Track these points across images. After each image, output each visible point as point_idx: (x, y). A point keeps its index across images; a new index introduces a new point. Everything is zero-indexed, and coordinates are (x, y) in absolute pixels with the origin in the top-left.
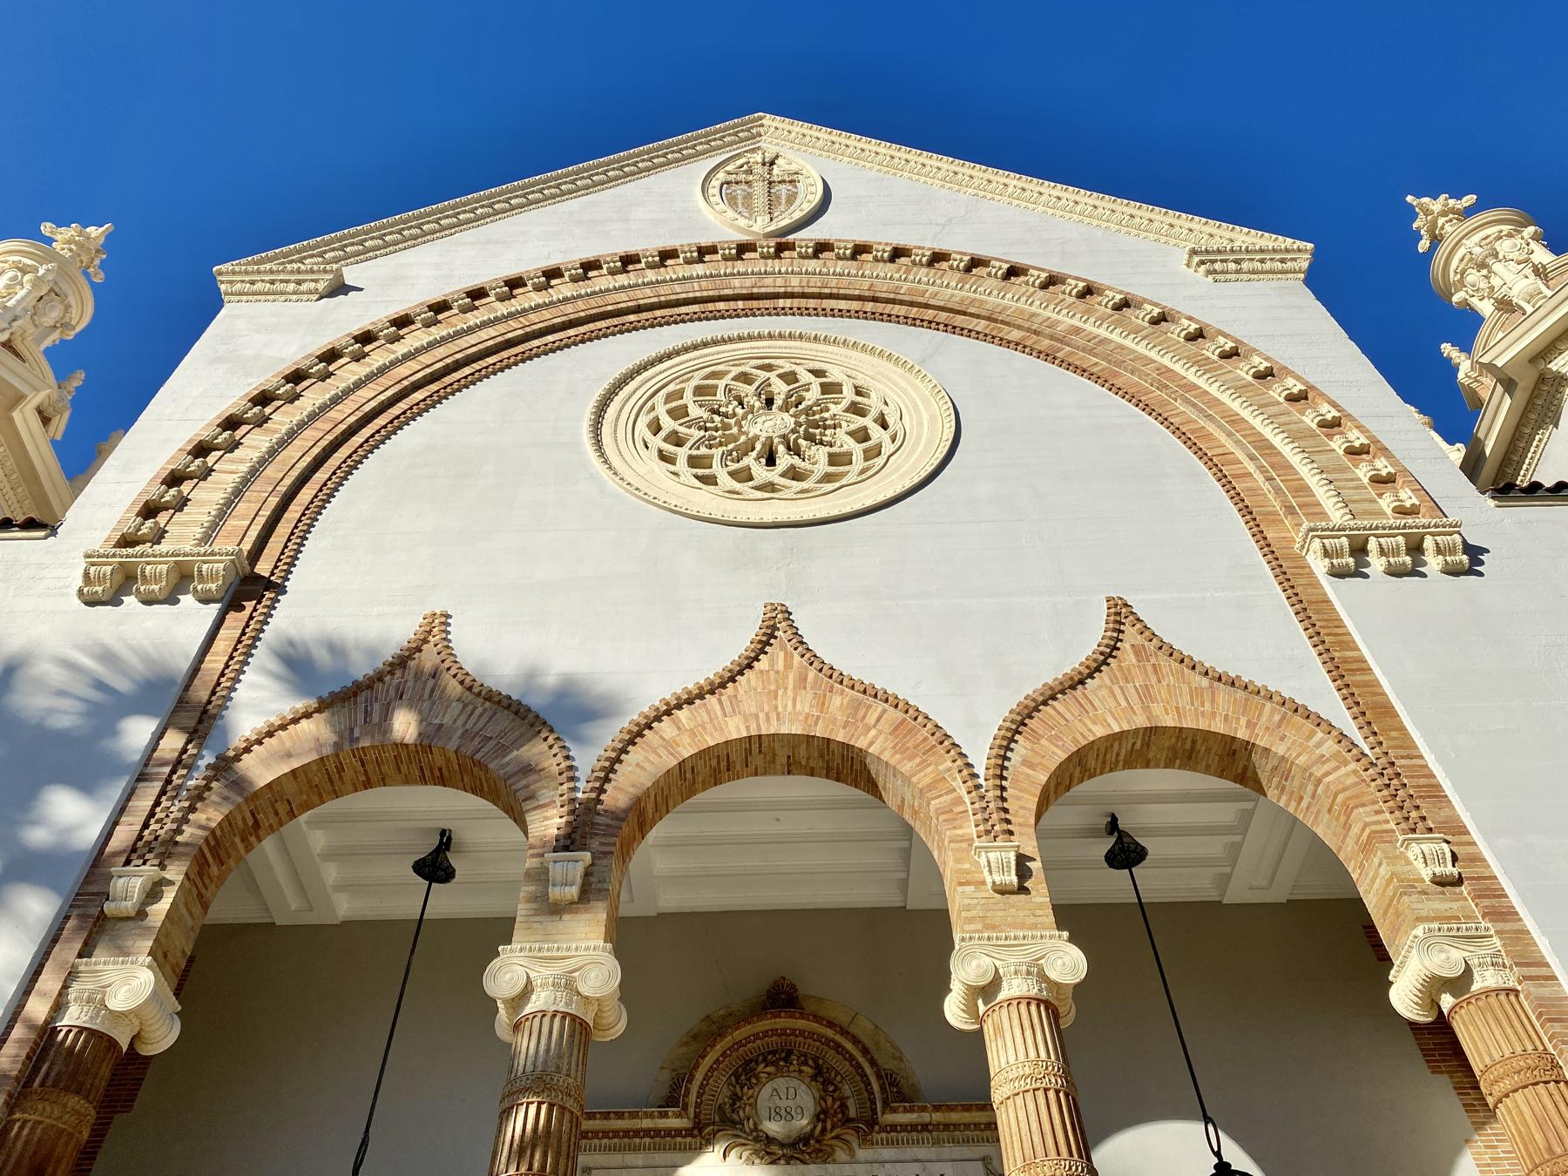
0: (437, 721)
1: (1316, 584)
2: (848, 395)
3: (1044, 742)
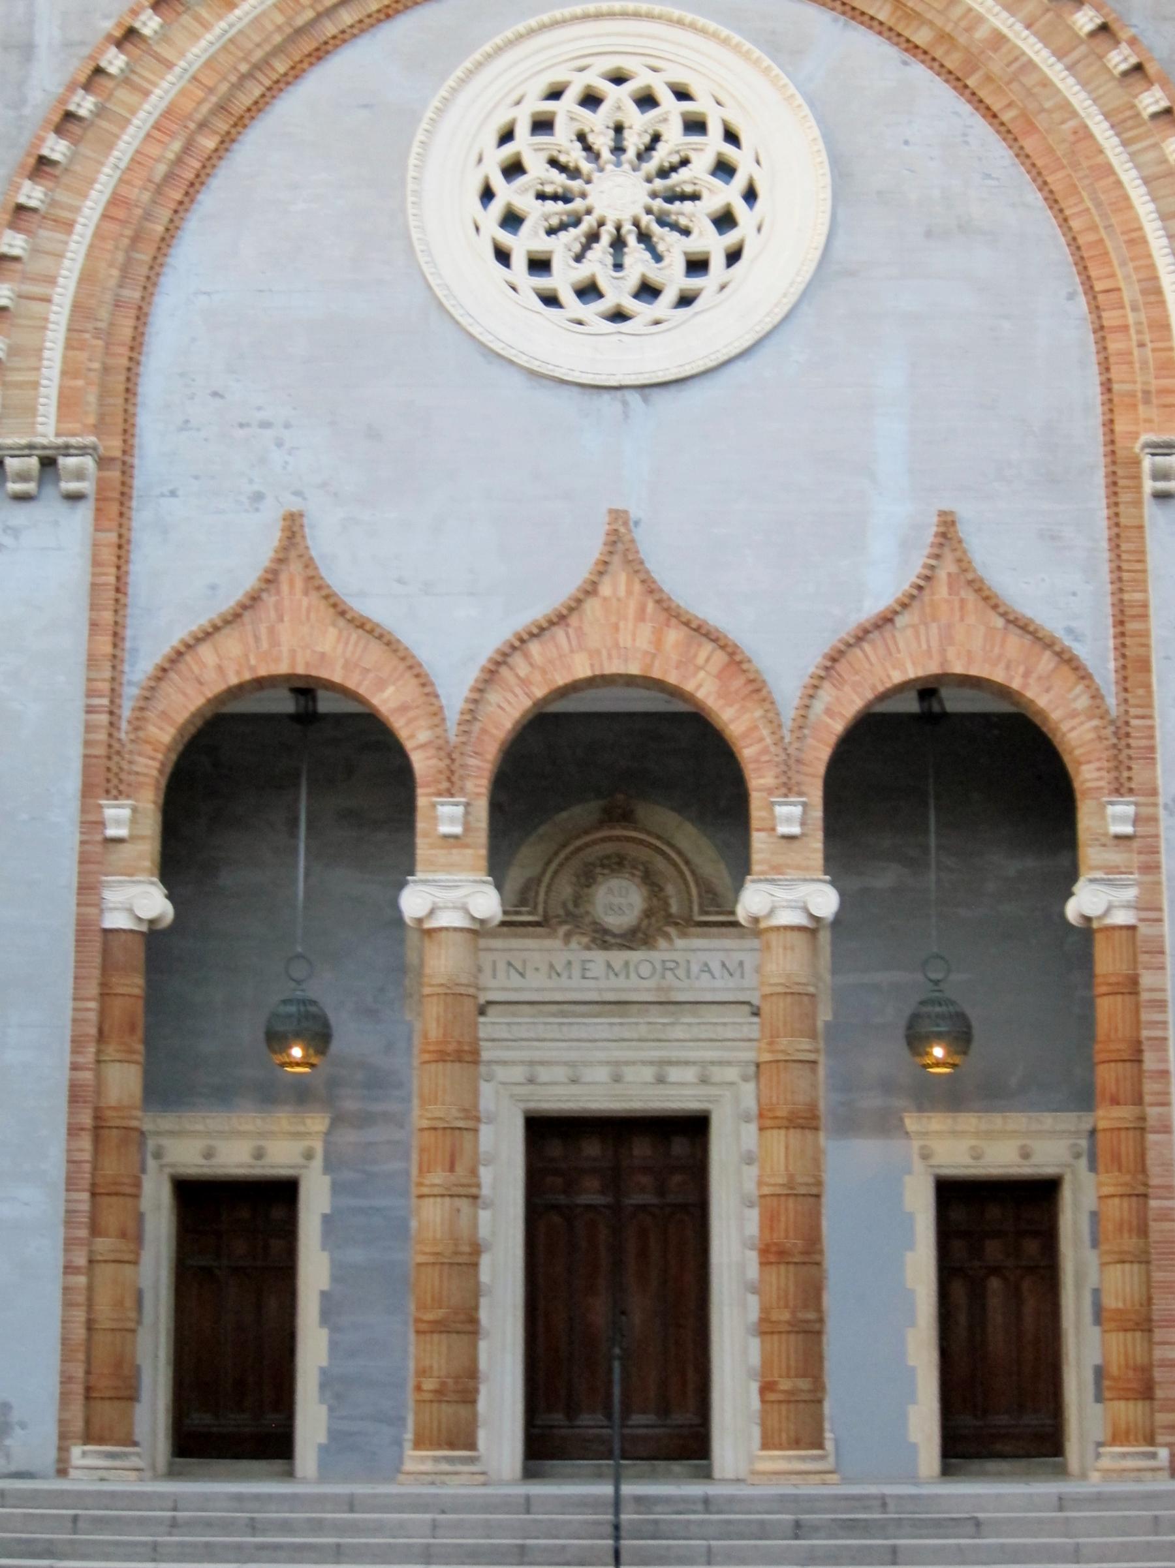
1: (1138, 503)
3: (847, 688)
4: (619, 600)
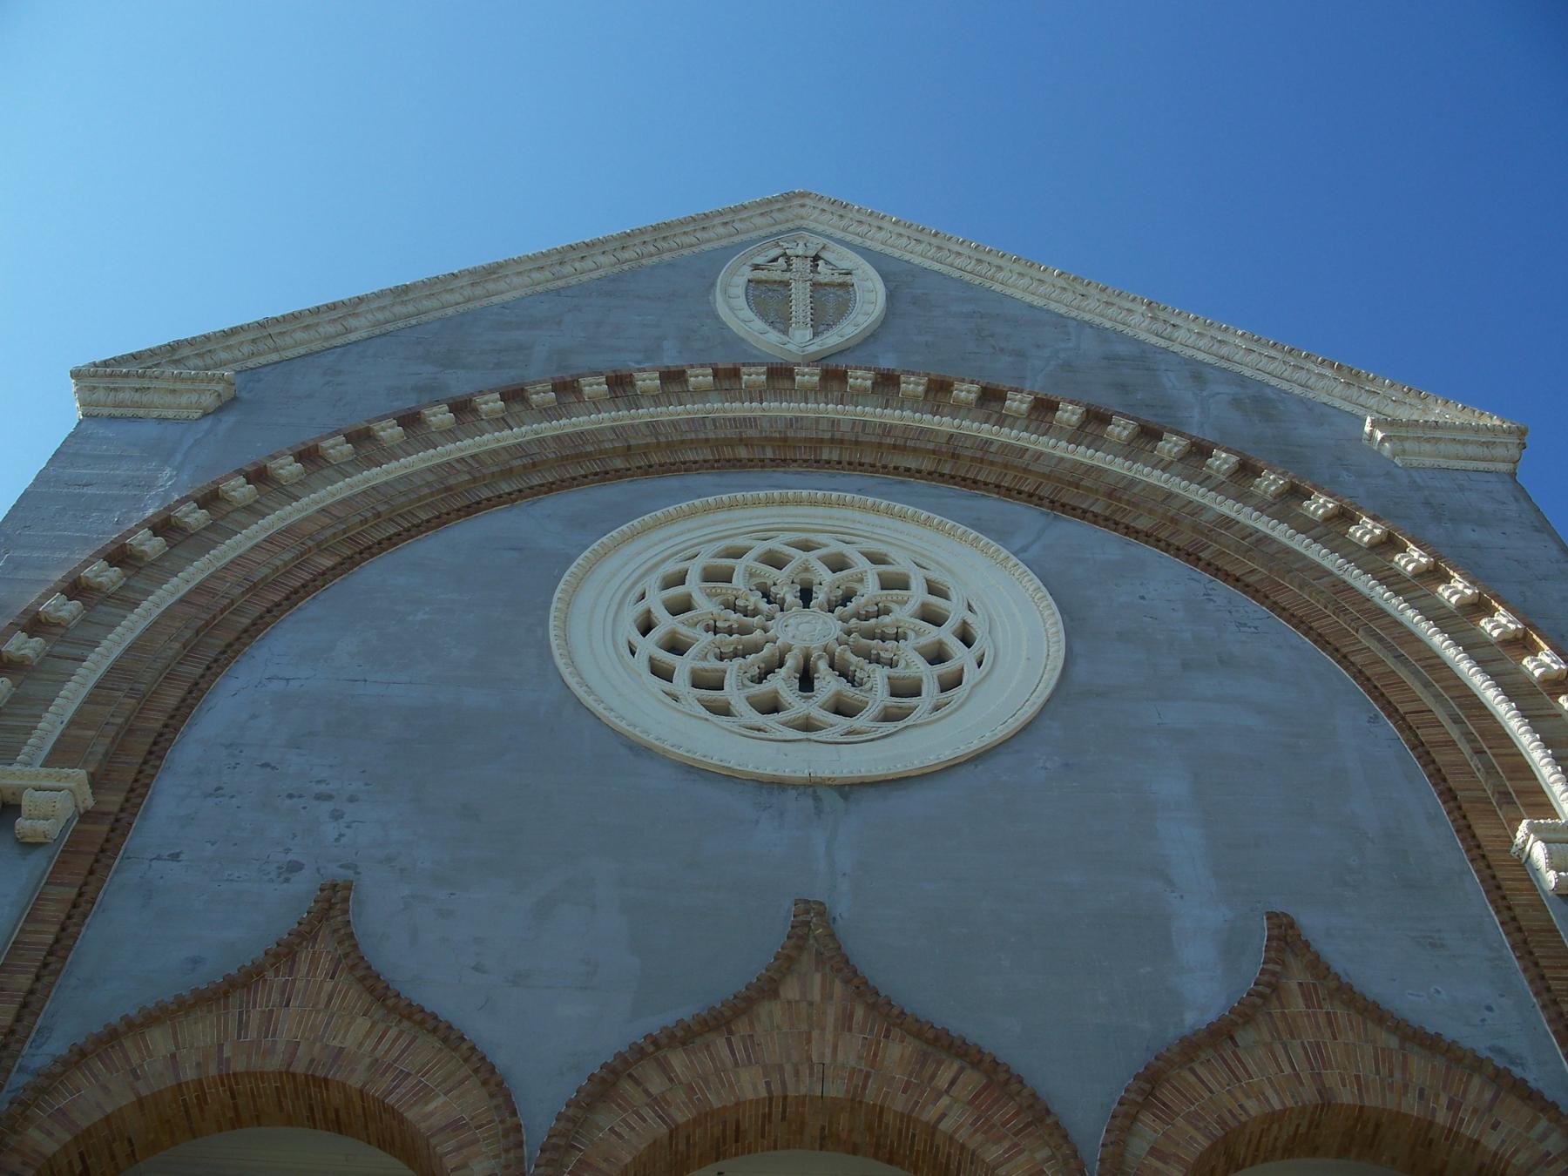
0: (336, 1043)
2: (918, 594)
3: (1180, 1121)
4: (811, 1004)
